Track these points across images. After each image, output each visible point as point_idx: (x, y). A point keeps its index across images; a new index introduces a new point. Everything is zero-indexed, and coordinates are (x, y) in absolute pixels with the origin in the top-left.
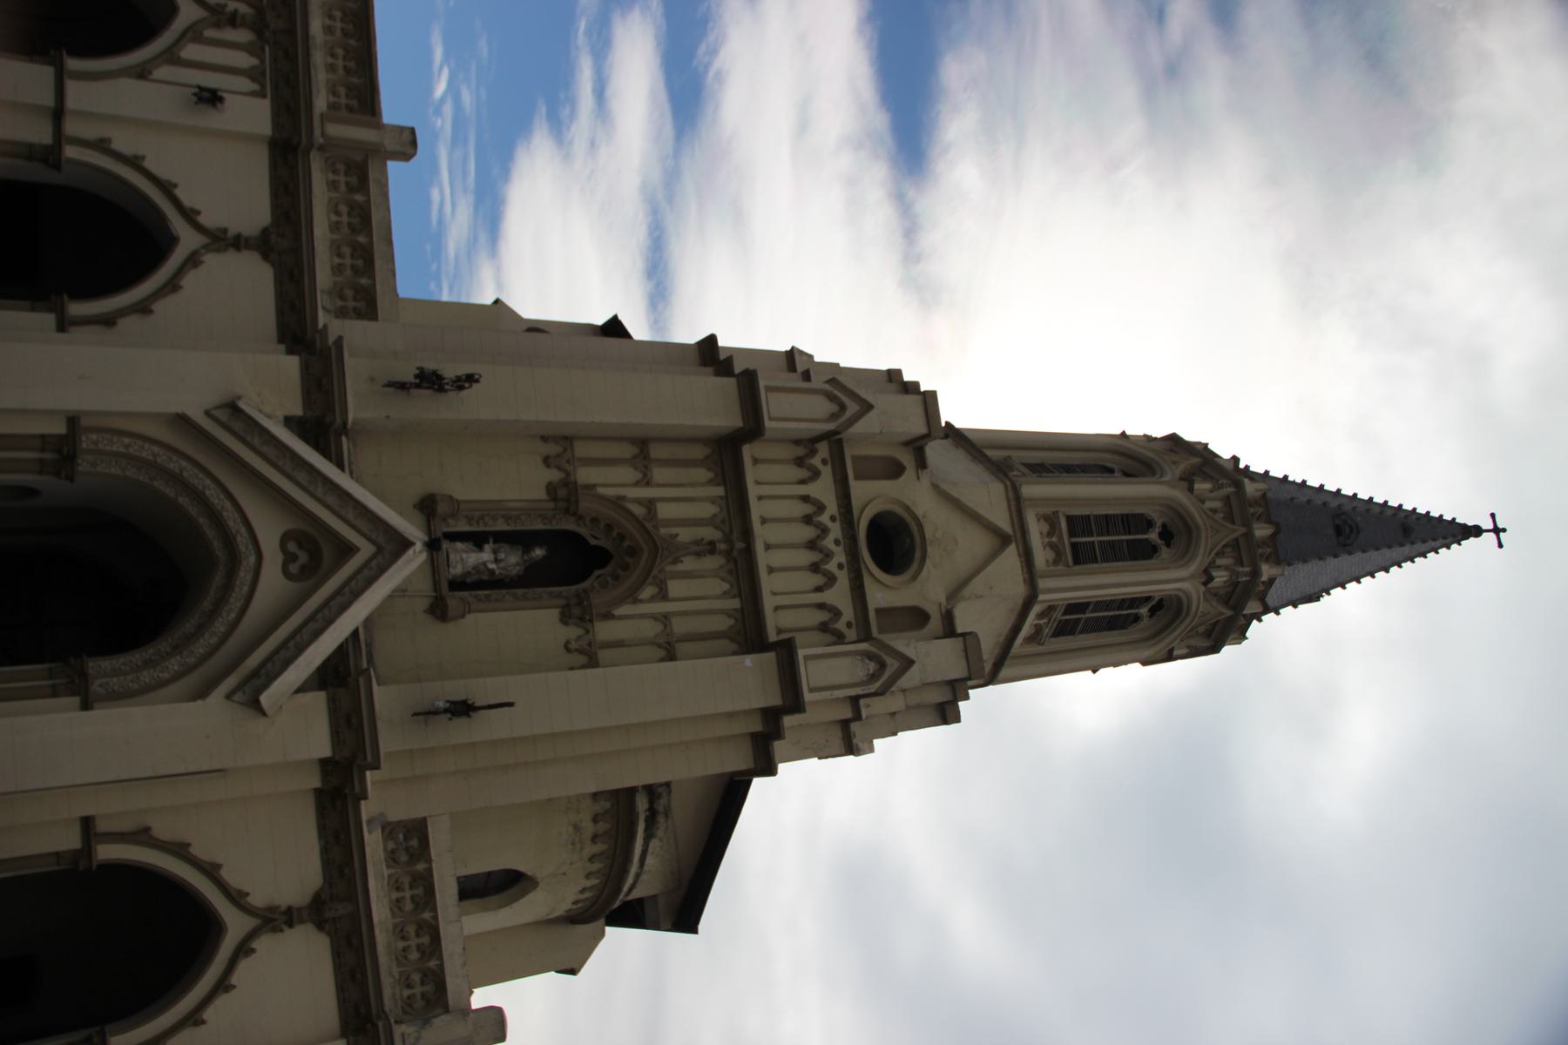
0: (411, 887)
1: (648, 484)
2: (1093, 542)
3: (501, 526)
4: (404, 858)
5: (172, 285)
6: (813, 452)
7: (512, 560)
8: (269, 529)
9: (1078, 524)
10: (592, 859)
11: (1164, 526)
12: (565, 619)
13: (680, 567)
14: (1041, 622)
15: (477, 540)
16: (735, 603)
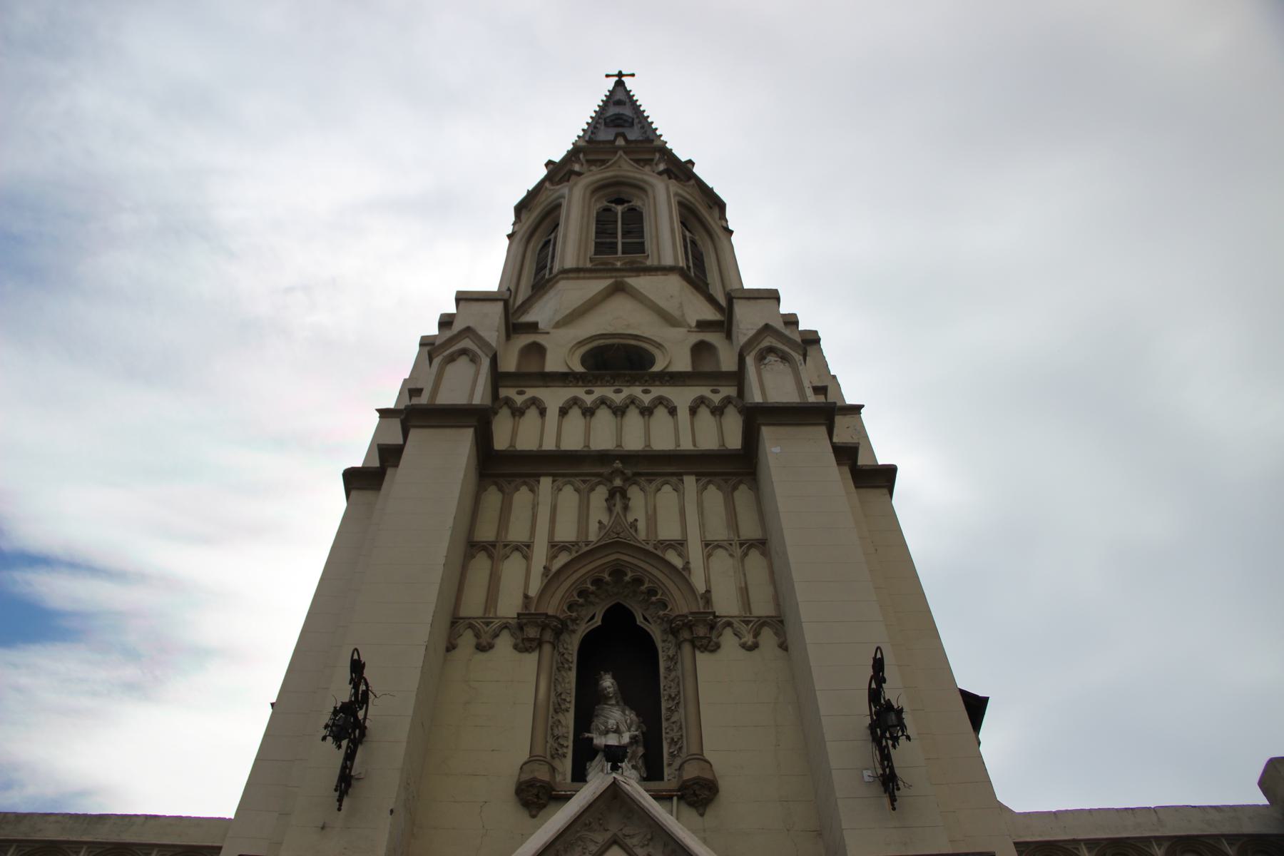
2: (623, 243)
3: (569, 719)
16: (690, 481)
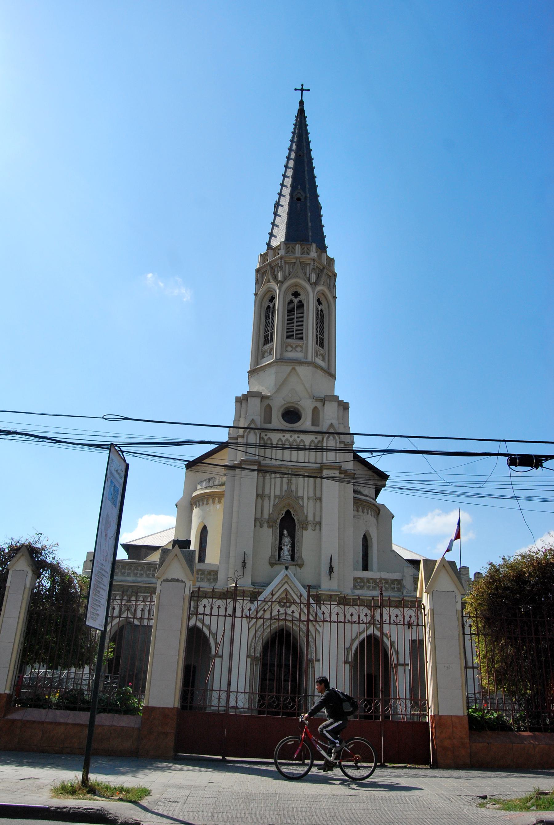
0: (370, 583)
1: (270, 497)
2: (296, 329)
3: (277, 542)
4: (362, 584)
6: (263, 438)
7: (287, 540)
9: (289, 336)
10: (363, 512)
11: (293, 295)
12: (306, 529)
13: (295, 491)
14: (319, 354)
15: (280, 549)
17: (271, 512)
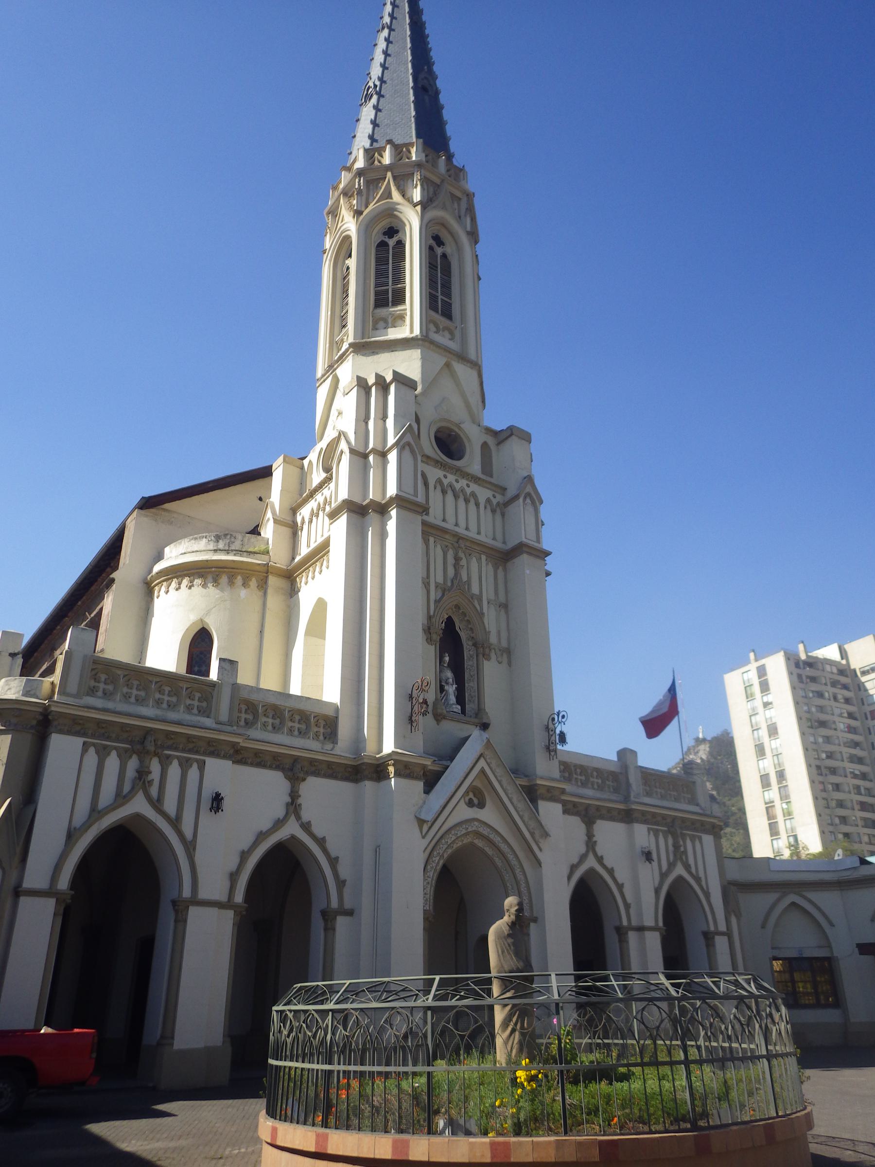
5: (321, 842)
8: (463, 813)
12: (488, 659)
17: (432, 613)
